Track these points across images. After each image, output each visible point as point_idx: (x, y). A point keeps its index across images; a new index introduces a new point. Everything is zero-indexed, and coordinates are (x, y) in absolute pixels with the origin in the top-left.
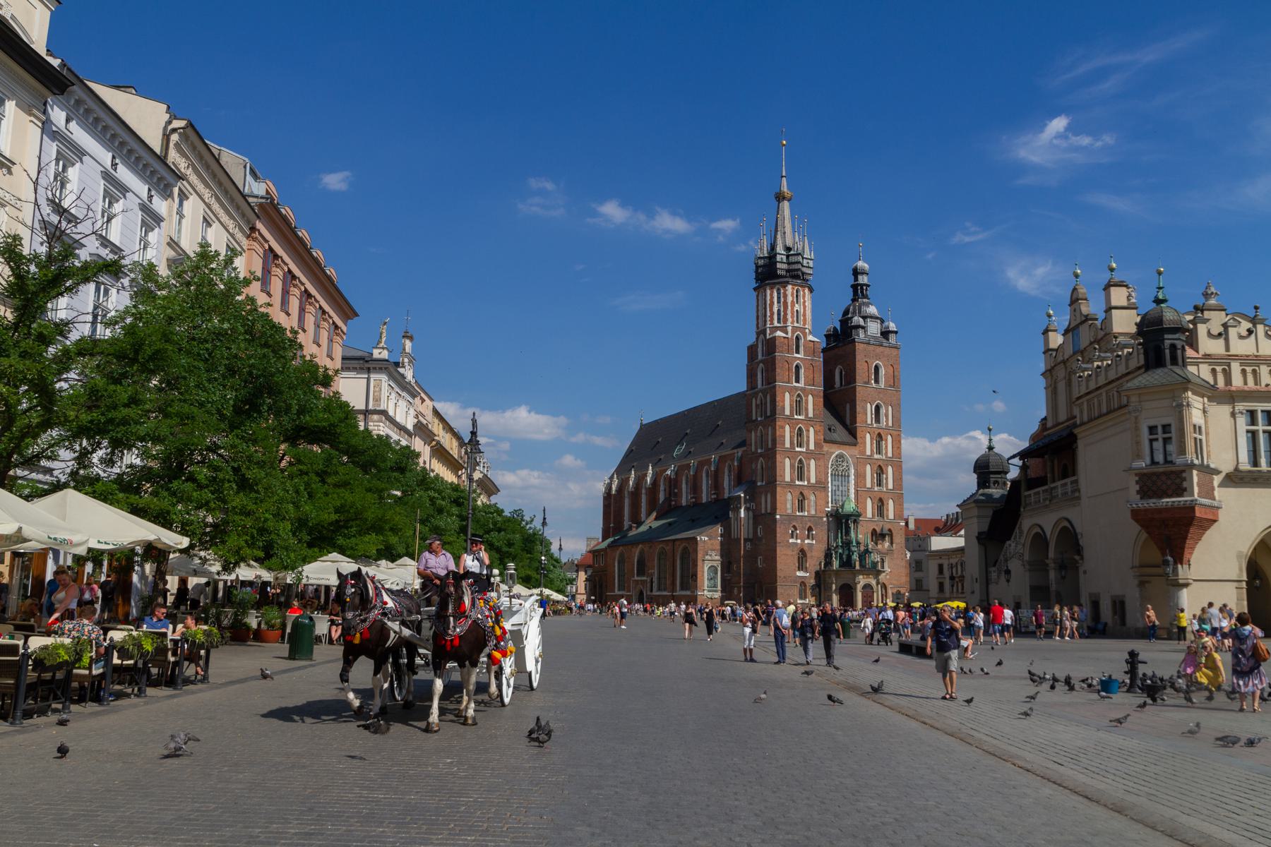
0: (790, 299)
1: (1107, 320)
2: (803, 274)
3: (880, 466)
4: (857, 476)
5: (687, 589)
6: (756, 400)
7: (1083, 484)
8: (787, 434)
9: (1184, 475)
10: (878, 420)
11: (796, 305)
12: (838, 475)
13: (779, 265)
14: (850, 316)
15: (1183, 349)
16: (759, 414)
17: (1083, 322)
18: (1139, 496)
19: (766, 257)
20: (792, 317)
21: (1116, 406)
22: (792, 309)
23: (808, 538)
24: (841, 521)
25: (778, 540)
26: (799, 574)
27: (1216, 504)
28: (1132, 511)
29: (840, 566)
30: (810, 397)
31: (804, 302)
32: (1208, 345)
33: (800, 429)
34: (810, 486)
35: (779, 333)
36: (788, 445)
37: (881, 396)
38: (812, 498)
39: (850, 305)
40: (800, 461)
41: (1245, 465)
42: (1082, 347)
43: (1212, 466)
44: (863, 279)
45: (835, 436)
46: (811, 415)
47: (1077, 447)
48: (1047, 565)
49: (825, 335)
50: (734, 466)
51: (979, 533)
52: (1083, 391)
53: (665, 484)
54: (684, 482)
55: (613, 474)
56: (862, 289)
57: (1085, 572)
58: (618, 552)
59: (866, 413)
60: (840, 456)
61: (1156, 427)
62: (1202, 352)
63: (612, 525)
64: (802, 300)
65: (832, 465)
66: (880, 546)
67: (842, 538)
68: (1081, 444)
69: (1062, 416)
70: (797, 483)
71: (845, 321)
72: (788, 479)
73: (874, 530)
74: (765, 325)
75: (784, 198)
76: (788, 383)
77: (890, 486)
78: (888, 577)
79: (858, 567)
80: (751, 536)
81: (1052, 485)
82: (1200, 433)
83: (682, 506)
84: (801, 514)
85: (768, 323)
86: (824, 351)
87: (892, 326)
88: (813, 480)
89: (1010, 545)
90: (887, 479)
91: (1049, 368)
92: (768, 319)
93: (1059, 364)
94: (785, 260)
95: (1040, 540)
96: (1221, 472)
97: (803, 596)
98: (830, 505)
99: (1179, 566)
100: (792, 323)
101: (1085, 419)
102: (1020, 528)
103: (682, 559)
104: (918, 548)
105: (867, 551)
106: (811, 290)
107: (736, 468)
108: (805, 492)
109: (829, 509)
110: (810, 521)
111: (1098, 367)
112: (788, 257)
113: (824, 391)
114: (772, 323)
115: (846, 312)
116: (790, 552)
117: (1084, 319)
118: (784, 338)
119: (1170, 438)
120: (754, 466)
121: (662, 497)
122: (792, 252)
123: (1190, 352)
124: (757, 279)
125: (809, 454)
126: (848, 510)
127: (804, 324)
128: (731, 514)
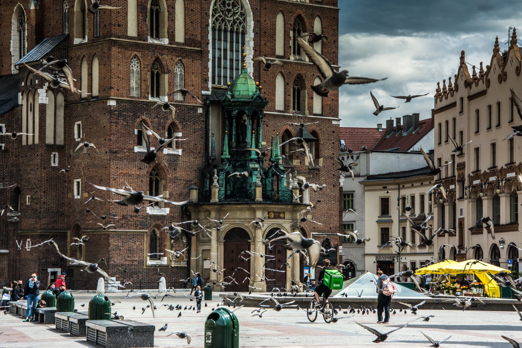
3: (299, 17)
4: (259, 32)
38: (178, 71)
50: (29, 11)
65: (215, 10)
67: (230, 147)
72: (132, 31)
80: (60, 141)
84: (156, 99)
88: (180, 37)
98: (210, 85)
107: (33, 15)
108: (166, 59)
109: (209, 93)
116: (135, 171)
120: (66, 8)
126: (242, 93)
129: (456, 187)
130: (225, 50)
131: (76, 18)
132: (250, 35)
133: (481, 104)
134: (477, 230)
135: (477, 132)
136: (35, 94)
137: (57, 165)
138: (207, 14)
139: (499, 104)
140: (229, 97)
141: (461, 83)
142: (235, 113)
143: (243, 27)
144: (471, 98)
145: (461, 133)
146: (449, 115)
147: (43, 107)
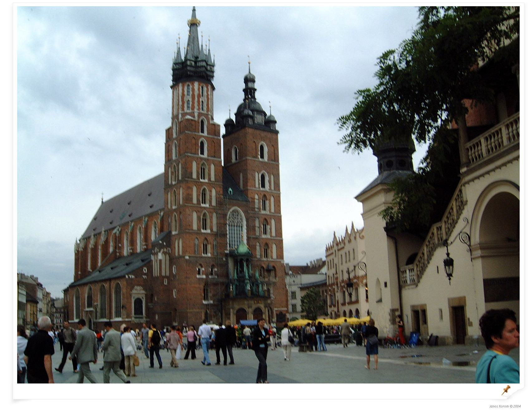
3: (265, 219)
6: (171, 169)
23: (212, 274)
30: (212, 167)
33: (204, 190)
40: (205, 215)
65: (229, 218)
72: (195, 227)
80: (168, 274)
83: (124, 256)
90: (271, 229)
98: (228, 248)
100: (199, 109)
109: (228, 252)
114: (183, 110)
118: (192, 120)
121: (111, 250)
129: (335, 287)
132: (245, 228)
133: (342, 252)
134: (344, 304)
135: (342, 264)
137: (166, 284)
139: (349, 252)
140: (236, 253)
141: (335, 245)
142: (239, 260)
143: (242, 224)
144: (338, 250)
145: (336, 265)
146: (331, 258)
147: (160, 261)
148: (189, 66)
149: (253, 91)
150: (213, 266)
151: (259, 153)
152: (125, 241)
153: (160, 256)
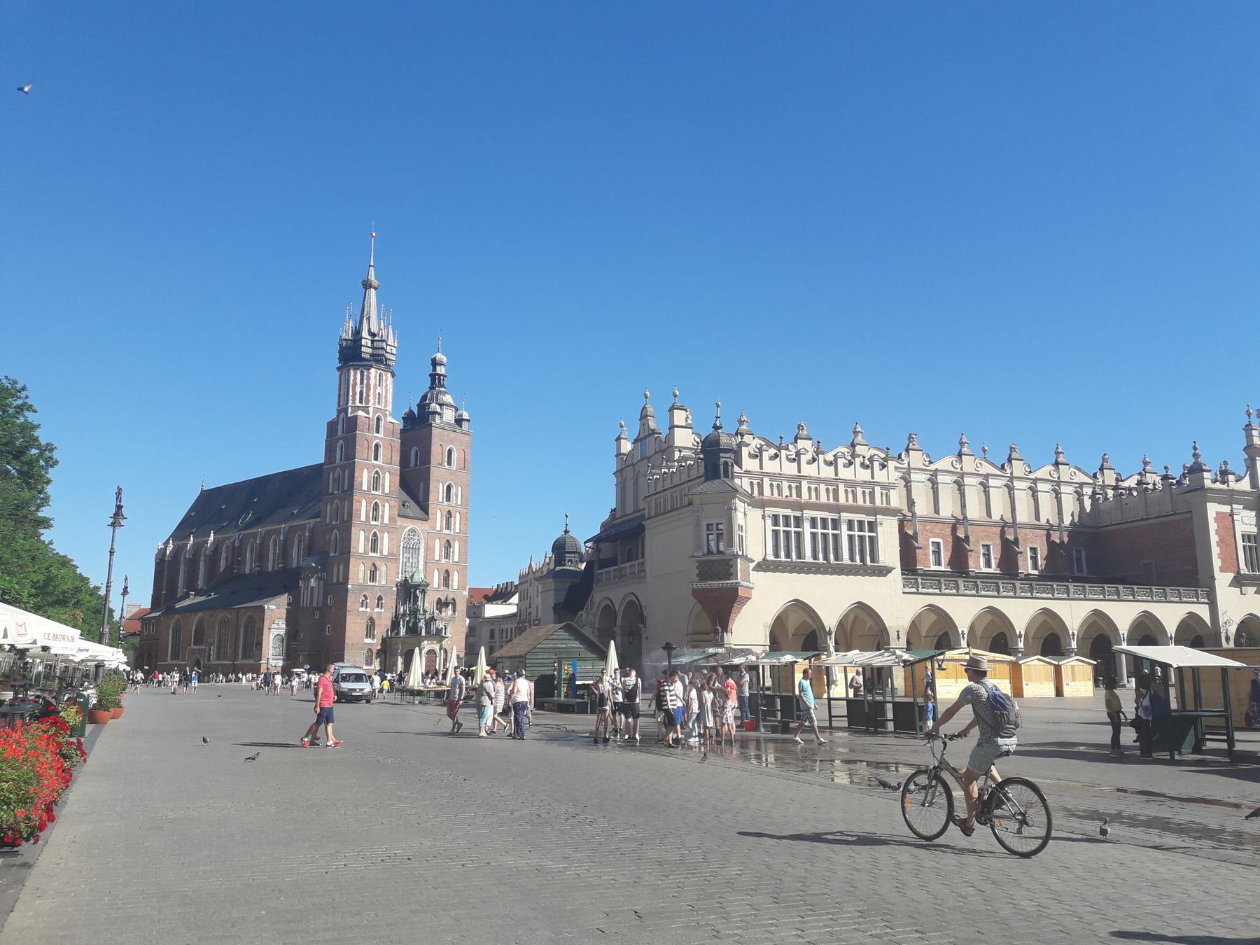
0: (372, 382)
1: (670, 436)
2: (387, 359)
3: (448, 541)
4: (427, 549)
5: (249, 658)
7: (648, 566)
8: (362, 508)
9: (731, 563)
10: (448, 499)
11: (379, 388)
12: (409, 548)
13: (363, 349)
14: (427, 402)
15: (733, 466)
16: (336, 486)
17: (650, 435)
18: (698, 578)
19: (349, 340)
20: (374, 399)
21: (678, 506)
22: (375, 388)
23: (378, 607)
24: (409, 591)
25: (348, 608)
26: (368, 641)
27: (751, 585)
28: (693, 589)
29: (406, 633)
31: (386, 386)
32: (749, 464)
33: (376, 504)
34: (383, 558)
35: (360, 413)
36: (363, 518)
37: (453, 477)
38: (384, 568)
39: (428, 392)
40: (375, 534)
41: (771, 557)
42: (649, 455)
43: (749, 556)
44: (441, 370)
45: (409, 512)
46: (387, 491)
47: (644, 536)
48: (615, 632)
49: (403, 418)
50: (304, 536)
51: (555, 604)
52: (652, 491)
53: (227, 552)
54: (248, 551)
55: (168, 540)
56: (439, 379)
57: (647, 638)
58: (173, 621)
59: (437, 492)
60: (413, 531)
61: (712, 525)
62: (744, 469)
63: (163, 592)
64: (384, 384)
65: (404, 538)
66: (443, 614)
68: (648, 534)
69: (630, 509)
70: (370, 554)
71: (423, 405)
72: (361, 550)
73: (439, 599)
74: (347, 403)
75: (371, 286)
76: (367, 460)
77: (456, 560)
78: (449, 642)
79: (423, 634)
80: (320, 605)
81: (622, 566)
82: (742, 531)
84: (372, 584)
85: (350, 402)
86: (402, 431)
87: (466, 416)
88: (385, 553)
89: (582, 615)
90: (453, 552)
91: (620, 468)
92: (350, 398)
93: (629, 466)
94: (369, 345)
95: (609, 611)
96: (754, 561)
97: (369, 662)
98: (400, 575)
99: (725, 634)
100: (374, 404)
101: (653, 514)
102: (591, 601)
103: (246, 628)
104: (474, 616)
105: (433, 619)
106: (393, 375)
107: (307, 538)
109: (399, 580)
110: (380, 590)
111: (665, 473)
112: (373, 342)
113: (401, 469)
115: (424, 398)
116: (359, 621)
117: (651, 432)
118: (366, 417)
119: (722, 534)
120: (327, 538)
121: (222, 565)
122: (377, 338)
123: (736, 469)
124: (340, 360)
125: (384, 528)
127: (386, 406)
128: (301, 583)
130: (409, 558)
131: (333, 543)
132: (422, 550)
136: (309, 582)
138: (400, 541)
142: (413, 590)
147: (312, 588)
148: (365, 346)
149: (442, 378)
150: (380, 598)
151: (446, 459)
152: (248, 554)
153: (313, 582)
